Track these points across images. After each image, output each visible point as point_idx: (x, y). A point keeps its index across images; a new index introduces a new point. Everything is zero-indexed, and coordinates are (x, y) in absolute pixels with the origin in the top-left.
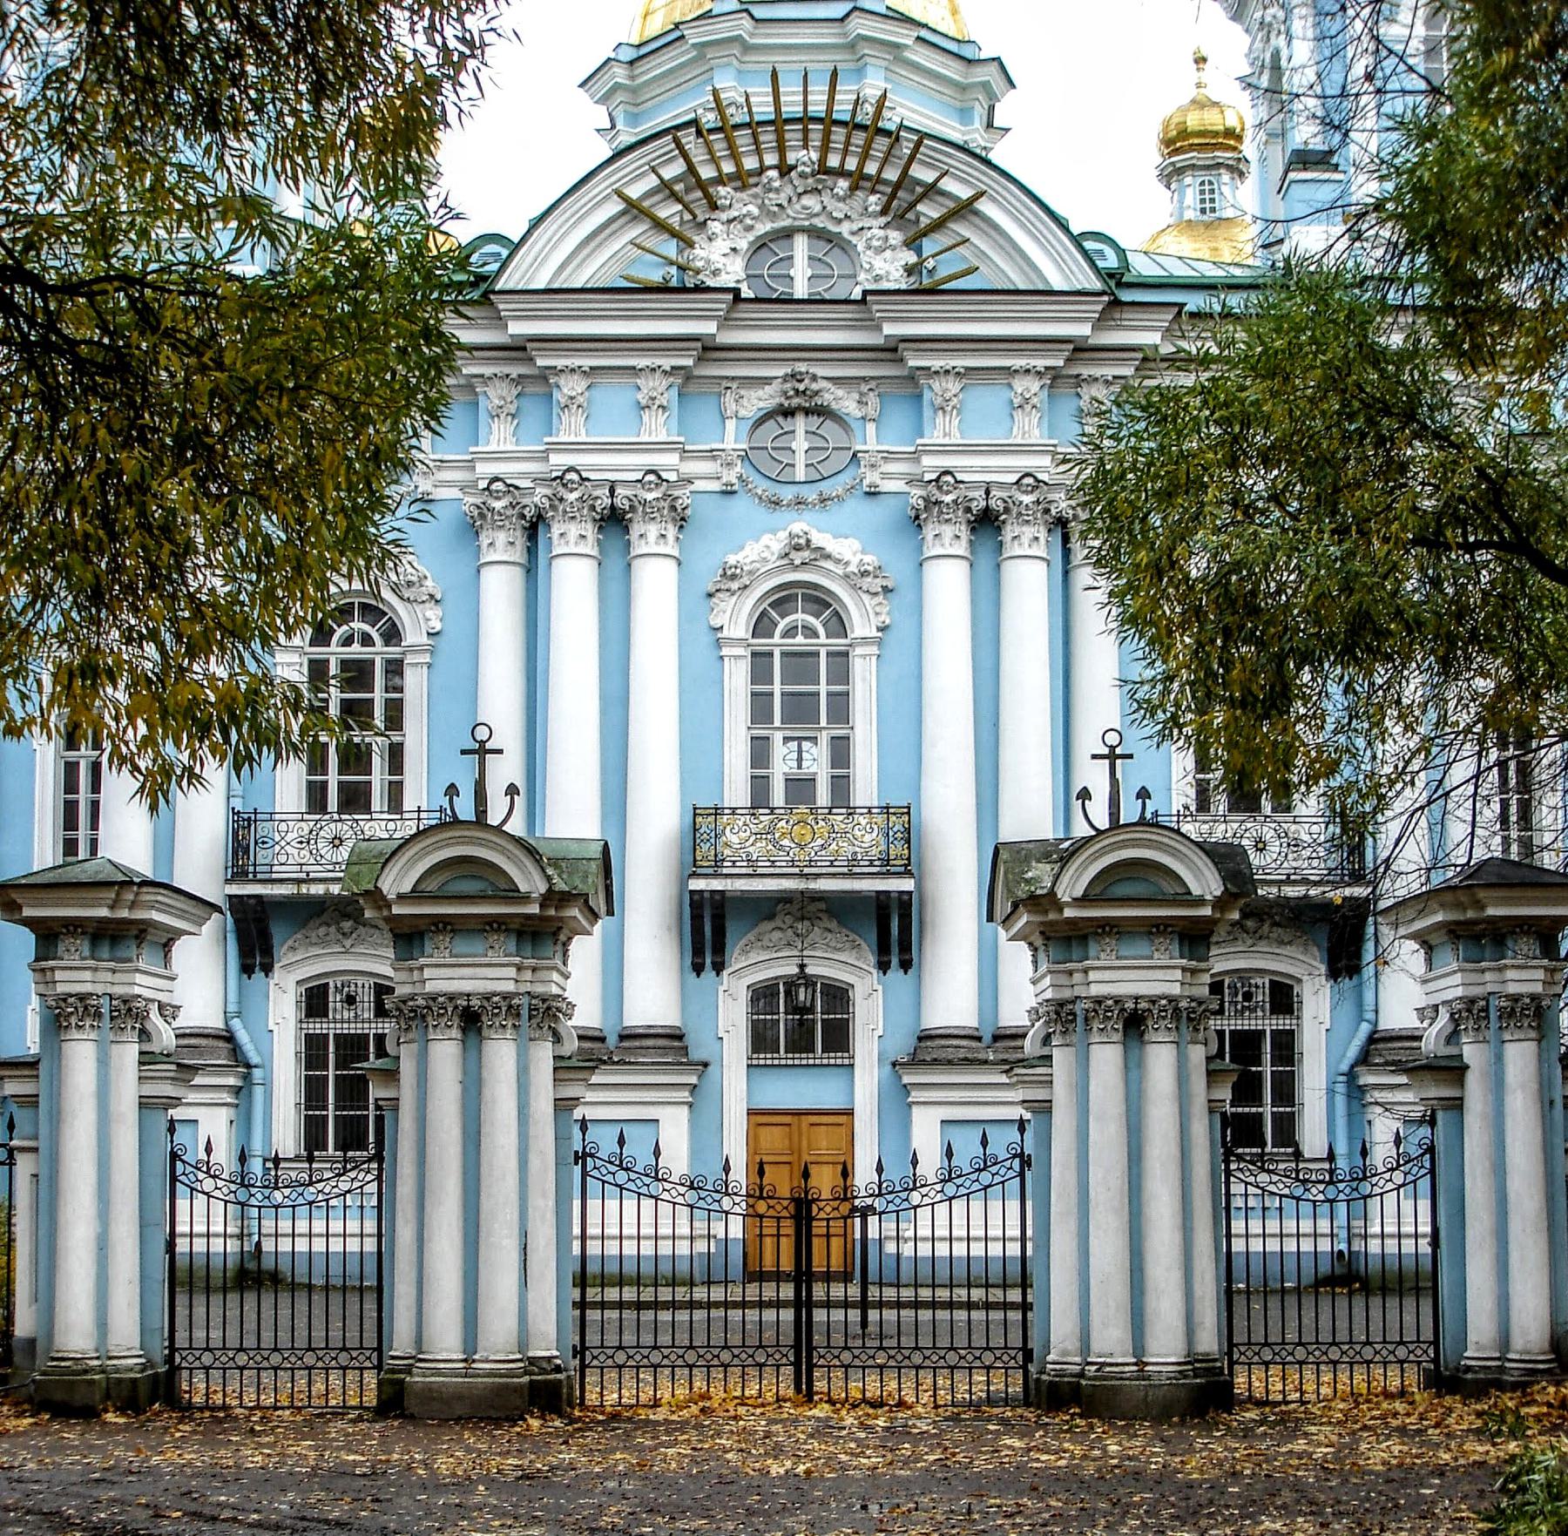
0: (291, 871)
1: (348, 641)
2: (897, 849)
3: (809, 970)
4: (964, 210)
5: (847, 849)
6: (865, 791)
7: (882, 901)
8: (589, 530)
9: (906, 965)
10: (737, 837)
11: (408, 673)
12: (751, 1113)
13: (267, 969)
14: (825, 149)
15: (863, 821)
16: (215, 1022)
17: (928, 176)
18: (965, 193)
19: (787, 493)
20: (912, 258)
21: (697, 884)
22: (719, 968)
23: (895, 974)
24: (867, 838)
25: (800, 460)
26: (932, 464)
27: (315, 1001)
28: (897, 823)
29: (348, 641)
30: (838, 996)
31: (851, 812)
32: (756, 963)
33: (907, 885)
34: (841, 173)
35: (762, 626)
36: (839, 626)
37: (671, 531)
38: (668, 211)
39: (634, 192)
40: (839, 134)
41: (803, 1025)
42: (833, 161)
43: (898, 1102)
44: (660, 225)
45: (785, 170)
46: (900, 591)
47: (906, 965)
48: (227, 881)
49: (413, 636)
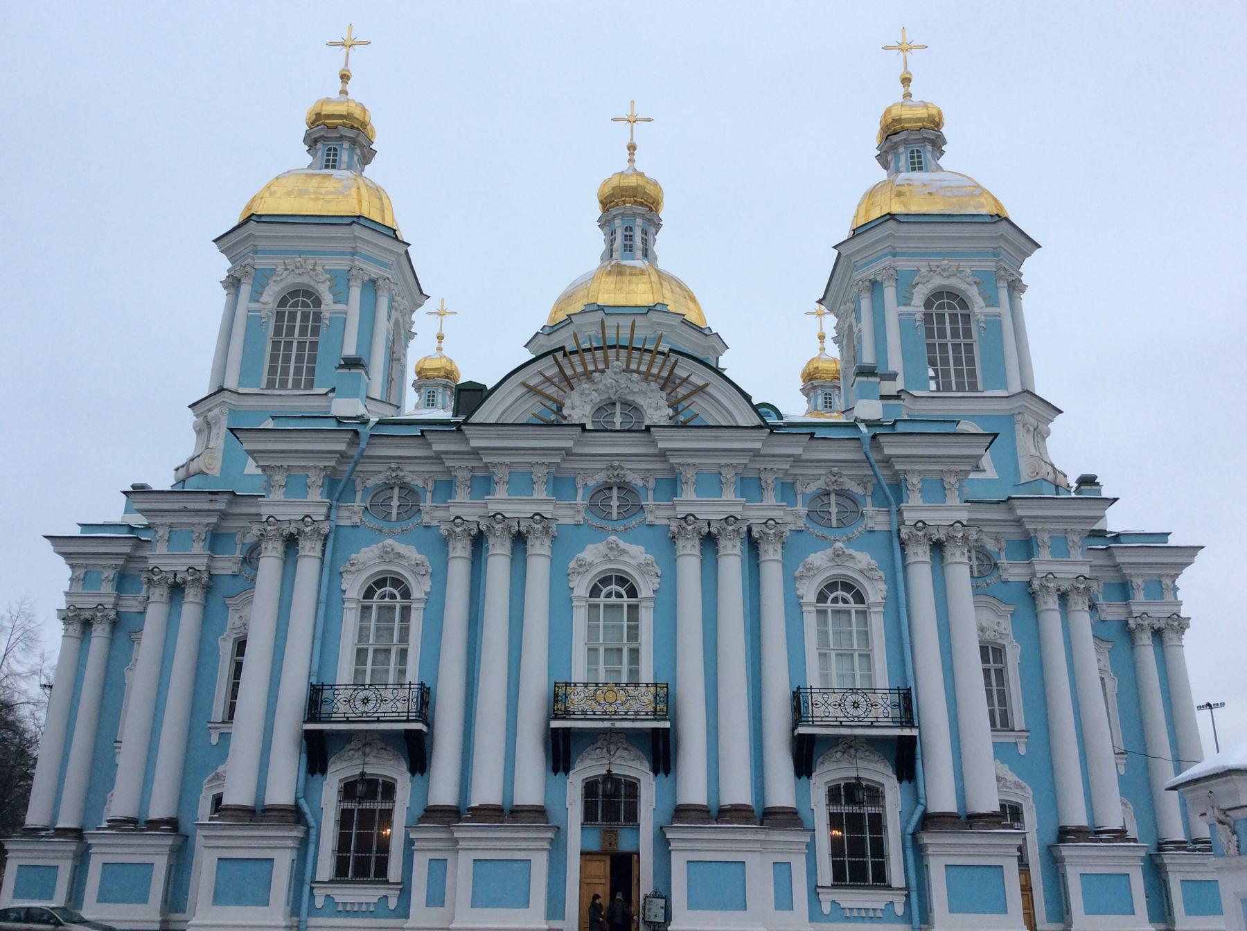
0: (339, 717)
1: (383, 597)
2: (661, 706)
3: (614, 771)
5: (635, 707)
6: (646, 675)
8: (508, 543)
9: (667, 772)
10: (578, 700)
11: (413, 613)
14: (628, 362)
15: (643, 690)
19: (608, 526)
21: (555, 724)
22: (567, 771)
23: (661, 775)
24: (646, 698)
25: (615, 511)
26: (682, 511)
27: (348, 790)
28: (662, 692)
30: (632, 788)
31: (637, 685)
32: (587, 768)
33: (667, 725)
35: (595, 592)
36: (632, 592)
37: (547, 542)
41: (610, 803)
42: (633, 367)
47: (667, 772)
48: (304, 722)
49: (416, 593)
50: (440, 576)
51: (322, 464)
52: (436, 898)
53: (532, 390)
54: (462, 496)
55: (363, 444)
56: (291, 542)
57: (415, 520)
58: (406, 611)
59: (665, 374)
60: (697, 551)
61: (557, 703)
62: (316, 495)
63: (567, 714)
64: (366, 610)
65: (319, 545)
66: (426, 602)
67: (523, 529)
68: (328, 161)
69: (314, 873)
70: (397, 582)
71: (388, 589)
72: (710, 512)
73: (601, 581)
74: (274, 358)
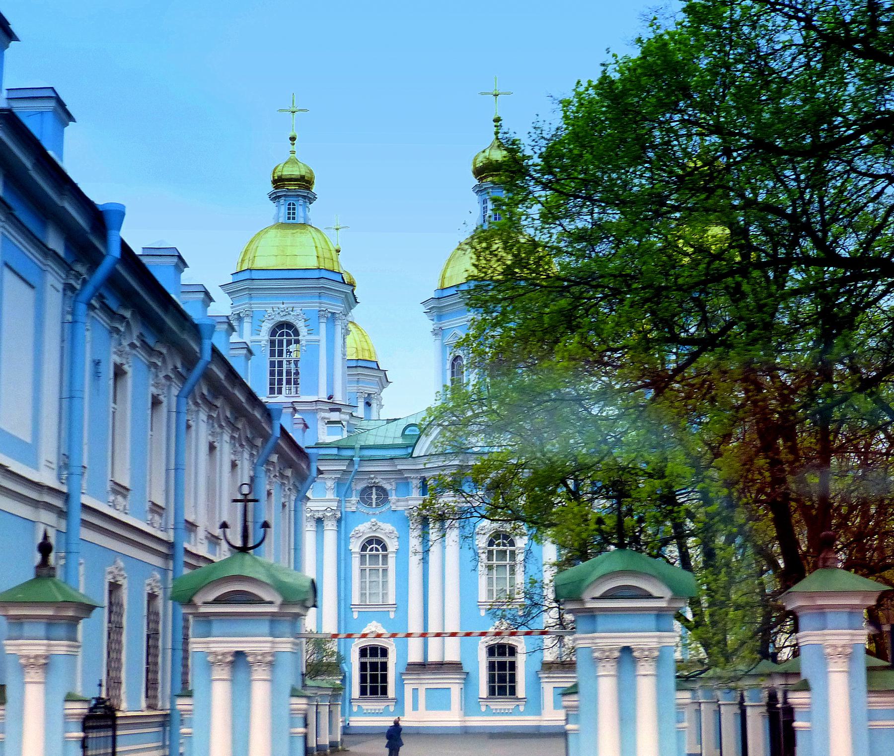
1: (371, 550)
29: (371, 550)
50: (403, 540)
51: (333, 476)
52: (415, 707)
55: (356, 466)
56: (319, 521)
57: (387, 507)
58: (385, 557)
62: (330, 495)
64: (363, 557)
65: (335, 523)
66: (396, 553)
68: (289, 214)
69: (350, 694)
70: (379, 541)
71: (374, 546)
73: (495, 537)
74: (272, 373)
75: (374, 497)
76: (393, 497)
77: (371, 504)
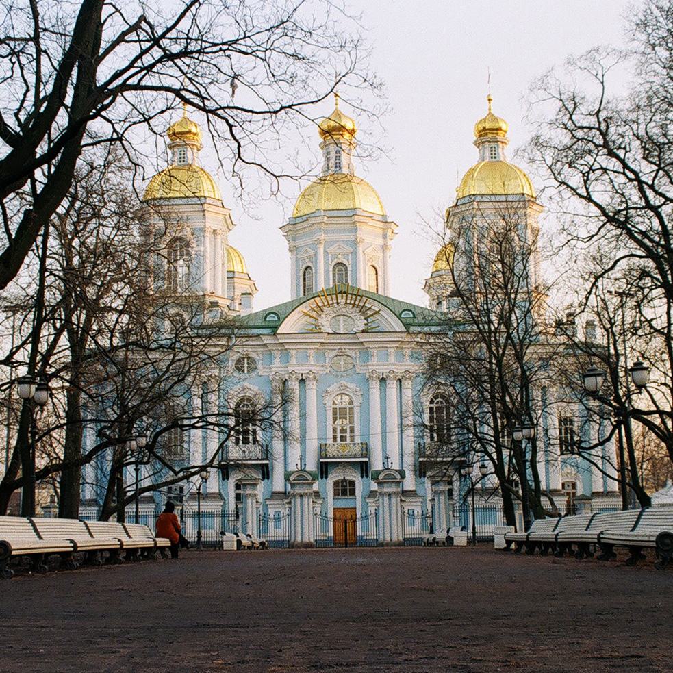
2: (365, 452)
4: (377, 313)
5: (354, 453)
6: (357, 440)
7: (361, 463)
10: (331, 450)
12: (334, 509)
13: (228, 479)
14: (347, 299)
16: (217, 491)
17: (370, 306)
18: (377, 310)
20: (366, 322)
21: (322, 460)
22: (326, 478)
24: (358, 450)
26: (371, 368)
30: (352, 483)
33: (367, 460)
34: (350, 304)
38: (313, 314)
39: (305, 311)
40: (349, 296)
43: (365, 505)
44: (311, 317)
45: (338, 303)
46: (366, 396)
53: (306, 314)
54: (277, 362)
59: (361, 304)
60: (378, 386)
61: (322, 450)
63: (326, 457)
67: (304, 378)
72: (383, 369)
75: (246, 365)
76: (260, 366)
77: (243, 371)
